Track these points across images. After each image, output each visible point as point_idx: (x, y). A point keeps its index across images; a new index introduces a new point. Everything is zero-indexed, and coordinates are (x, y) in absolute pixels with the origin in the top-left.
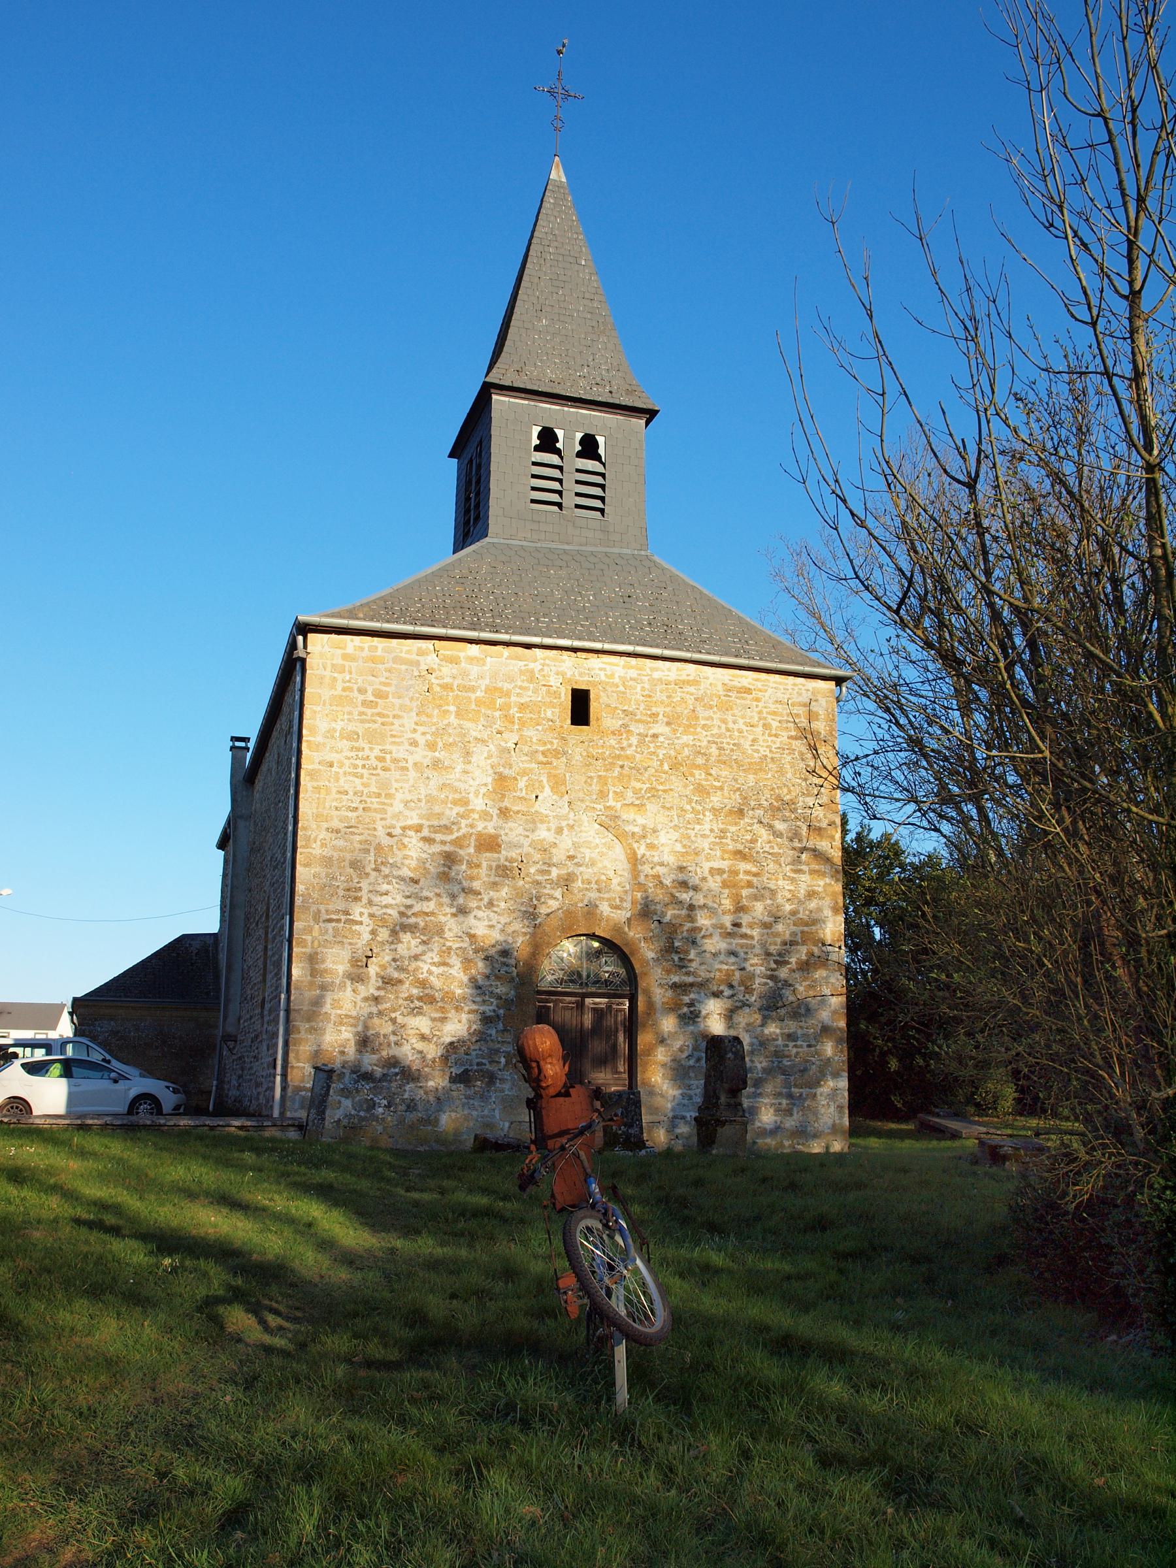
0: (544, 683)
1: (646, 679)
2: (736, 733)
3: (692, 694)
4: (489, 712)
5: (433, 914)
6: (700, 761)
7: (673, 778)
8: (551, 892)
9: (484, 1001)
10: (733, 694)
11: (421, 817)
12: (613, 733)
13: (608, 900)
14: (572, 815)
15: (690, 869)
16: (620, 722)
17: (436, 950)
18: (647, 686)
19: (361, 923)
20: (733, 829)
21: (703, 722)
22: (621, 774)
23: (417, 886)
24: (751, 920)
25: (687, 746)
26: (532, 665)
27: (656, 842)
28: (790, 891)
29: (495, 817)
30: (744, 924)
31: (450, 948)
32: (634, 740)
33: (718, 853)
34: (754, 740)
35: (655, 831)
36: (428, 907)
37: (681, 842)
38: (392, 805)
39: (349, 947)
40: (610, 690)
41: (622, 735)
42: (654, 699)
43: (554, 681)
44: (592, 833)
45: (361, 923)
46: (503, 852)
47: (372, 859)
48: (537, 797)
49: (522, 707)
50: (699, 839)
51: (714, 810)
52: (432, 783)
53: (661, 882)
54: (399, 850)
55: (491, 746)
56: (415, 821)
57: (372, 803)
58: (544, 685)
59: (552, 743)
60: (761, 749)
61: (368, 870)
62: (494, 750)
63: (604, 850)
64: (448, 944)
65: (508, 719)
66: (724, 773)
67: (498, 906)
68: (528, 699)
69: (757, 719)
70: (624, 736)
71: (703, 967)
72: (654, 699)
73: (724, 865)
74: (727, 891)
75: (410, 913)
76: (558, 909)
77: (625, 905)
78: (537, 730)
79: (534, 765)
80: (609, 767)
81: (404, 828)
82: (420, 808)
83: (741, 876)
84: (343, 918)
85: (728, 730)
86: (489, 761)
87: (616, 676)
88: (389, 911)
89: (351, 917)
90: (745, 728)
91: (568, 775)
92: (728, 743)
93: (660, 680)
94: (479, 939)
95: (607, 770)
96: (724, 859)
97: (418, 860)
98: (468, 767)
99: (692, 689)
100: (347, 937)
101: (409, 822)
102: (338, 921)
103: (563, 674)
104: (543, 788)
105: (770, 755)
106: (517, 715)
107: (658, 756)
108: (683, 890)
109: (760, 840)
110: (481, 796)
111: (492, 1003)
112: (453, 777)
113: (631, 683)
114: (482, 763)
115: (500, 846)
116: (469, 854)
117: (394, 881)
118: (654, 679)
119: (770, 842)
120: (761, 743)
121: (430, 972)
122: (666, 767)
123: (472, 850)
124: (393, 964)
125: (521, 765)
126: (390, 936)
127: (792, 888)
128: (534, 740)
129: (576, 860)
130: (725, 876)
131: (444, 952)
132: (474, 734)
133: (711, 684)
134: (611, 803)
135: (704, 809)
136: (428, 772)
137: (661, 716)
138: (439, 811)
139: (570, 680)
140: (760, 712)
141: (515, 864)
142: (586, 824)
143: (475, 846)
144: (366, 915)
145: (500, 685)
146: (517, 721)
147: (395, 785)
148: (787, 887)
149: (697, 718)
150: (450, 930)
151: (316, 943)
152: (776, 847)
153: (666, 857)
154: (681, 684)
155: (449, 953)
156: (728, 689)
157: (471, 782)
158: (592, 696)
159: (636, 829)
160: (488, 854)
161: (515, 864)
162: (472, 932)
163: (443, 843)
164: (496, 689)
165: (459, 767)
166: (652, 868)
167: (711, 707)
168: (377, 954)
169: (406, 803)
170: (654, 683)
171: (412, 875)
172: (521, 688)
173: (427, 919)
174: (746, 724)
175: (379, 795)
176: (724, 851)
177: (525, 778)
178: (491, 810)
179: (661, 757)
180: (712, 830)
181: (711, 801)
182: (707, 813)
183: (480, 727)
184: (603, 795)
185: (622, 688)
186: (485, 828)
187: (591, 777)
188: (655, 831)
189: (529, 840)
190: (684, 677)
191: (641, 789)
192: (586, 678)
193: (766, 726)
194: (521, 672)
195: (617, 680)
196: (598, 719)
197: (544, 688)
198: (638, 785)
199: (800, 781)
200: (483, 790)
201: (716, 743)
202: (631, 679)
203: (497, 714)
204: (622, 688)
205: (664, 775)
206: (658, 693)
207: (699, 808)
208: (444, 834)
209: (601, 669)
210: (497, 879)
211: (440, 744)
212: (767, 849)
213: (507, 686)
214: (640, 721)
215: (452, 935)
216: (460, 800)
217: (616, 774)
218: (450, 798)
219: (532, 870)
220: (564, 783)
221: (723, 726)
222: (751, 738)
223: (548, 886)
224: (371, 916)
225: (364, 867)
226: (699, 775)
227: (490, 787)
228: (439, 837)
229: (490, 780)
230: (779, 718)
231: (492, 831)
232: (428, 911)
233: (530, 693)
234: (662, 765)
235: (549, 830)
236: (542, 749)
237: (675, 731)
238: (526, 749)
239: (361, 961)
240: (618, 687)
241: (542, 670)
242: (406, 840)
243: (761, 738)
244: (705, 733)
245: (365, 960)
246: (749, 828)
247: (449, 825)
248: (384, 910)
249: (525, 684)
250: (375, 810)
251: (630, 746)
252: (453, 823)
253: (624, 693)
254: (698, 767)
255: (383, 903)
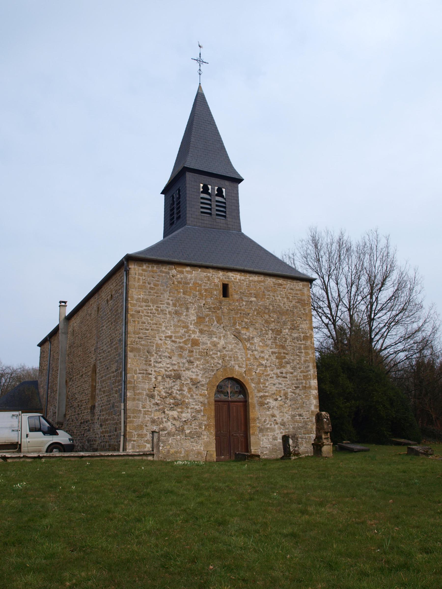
0: (213, 281)
1: (247, 280)
2: (278, 301)
3: (263, 286)
4: (195, 292)
5: (177, 370)
6: (267, 311)
7: (258, 317)
8: (218, 361)
9: (196, 404)
10: (276, 286)
11: (171, 332)
12: (237, 300)
13: (238, 364)
14: (224, 332)
15: (265, 352)
16: (239, 297)
17: (178, 384)
18: (248, 283)
19: (151, 374)
20: (279, 337)
21: (267, 297)
22: (240, 316)
23: (171, 360)
24: (286, 371)
25: (262, 305)
26: (209, 274)
27: (253, 342)
28: (298, 360)
29: (198, 333)
30: (284, 373)
31: (183, 384)
32: (244, 303)
33: (274, 346)
34: (284, 303)
35: (253, 338)
36: (175, 368)
37: (262, 342)
38: (161, 328)
39: (147, 384)
40: (235, 284)
41: (240, 301)
42: (250, 288)
43: (216, 281)
44: (231, 338)
45: (151, 374)
46: (201, 346)
47: (154, 348)
48: (212, 324)
49: (206, 290)
50: (268, 341)
51: (271, 330)
52: (175, 319)
53: (256, 357)
54: (164, 345)
55: (196, 305)
56: (170, 334)
57: (154, 327)
58: (213, 282)
59: (216, 304)
60: (287, 307)
61: (153, 353)
62: (196, 307)
63: (236, 345)
64: (183, 382)
65: (201, 294)
66: (275, 316)
67: (200, 367)
68: (208, 287)
69: (284, 295)
70: (241, 301)
71: (271, 389)
72: (250, 288)
73: (276, 350)
74: (277, 360)
75: (169, 370)
76: (221, 368)
77: (243, 366)
78: (211, 299)
79: (210, 313)
80: (237, 313)
81: (166, 337)
82: (171, 329)
83: (282, 355)
84: (145, 372)
85: (275, 299)
86: (195, 311)
87: (237, 279)
88: (161, 369)
89: (148, 372)
90: (281, 299)
91: (222, 316)
92: (276, 305)
93: (252, 280)
94: (194, 380)
95: (236, 315)
96: (276, 348)
97: (171, 349)
98: (188, 313)
99: (263, 284)
100: (146, 380)
101: (167, 335)
102: (143, 373)
103: (219, 278)
104: (214, 321)
105: (289, 309)
106: (204, 293)
107: (252, 309)
108: (263, 360)
109: (288, 341)
110: (192, 324)
111: (199, 405)
112: (182, 318)
113: (242, 282)
114: (193, 312)
115: (200, 344)
116: (189, 347)
117: (163, 357)
118: (250, 280)
119: (291, 342)
120: (286, 304)
121: (177, 393)
122: (255, 313)
123: (190, 345)
124: (163, 390)
125: (206, 312)
126: (162, 379)
127: (299, 359)
128: (210, 303)
129: (226, 349)
130: (277, 354)
131: (181, 385)
132: (189, 300)
133: (269, 282)
134: (238, 327)
135: (269, 329)
136: (174, 316)
137: (253, 294)
138: (178, 330)
139: (222, 280)
140: (286, 293)
141: (205, 351)
142: (229, 335)
143: (191, 344)
144: (153, 371)
145: (198, 282)
146: (204, 296)
147: (162, 320)
148: (298, 359)
149: (265, 295)
150: (183, 376)
151: (136, 382)
152: (293, 343)
153: (257, 347)
154: (260, 282)
155: (183, 386)
156: (275, 284)
157: (189, 319)
158: (230, 286)
159: (246, 337)
160: (196, 347)
161: (205, 351)
162: (191, 377)
163: (180, 343)
164: (197, 283)
165: (184, 314)
166: (252, 352)
167: (269, 291)
168: (158, 386)
169: (166, 327)
170: (250, 282)
171: (169, 355)
172: (205, 283)
173: (175, 372)
174: (281, 297)
175: (156, 324)
176: (276, 345)
177: (208, 318)
178: (196, 330)
179: (253, 309)
180: (272, 337)
181: (271, 326)
182: (270, 331)
183: (191, 298)
184: (235, 324)
185: (239, 284)
186: (194, 337)
187: (230, 317)
188: (253, 338)
189: (210, 341)
190: (260, 279)
191: (247, 322)
192: (227, 280)
193: (288, 298)
194: (205, 277)
195: (238, 280)
196: (232, 295)
197: (213, 283)
198: (246, 320)
199: (300, 319)
200: (193, 322)
201: (272, 304)
202: (243, 280)
203: (197, 293)
204: (239, 284)
205: (255, 317)
206: (252, 286)
207: (267, 329)
208: (180, 339)
209: (232, 276)
210: (199, 356)
211: (178, 305)
212: (290, 344)
213: (200, 282)
214: (246, 296)
215: (184, 378)
216: (185, 326)
217: (239, 316)
218: (182, 325)
219: (211, 353)
220: (221, 319)
221: (274, 298)
222: (283, 302)
223: (217, 359)
224: (155, 371)
225: (152, 352)
226: (267, 316)
227: (196, 321)
228: (178, 340)
229: (195, 318)
230: (292, 295)
231: (197, 338)
232: (175, 369)
233: (208, 285)
234: (254, 312)
235: (216, 337)
236: (213, 306)
237: (258, 300)
238: (208, 307)
239: (152, 389)
240: (238, 283)
241: (212, 276)
242: (167, 342)
243: (286, 302)
244: (268, 301)
245: (153, 388)
246: (284, 336)
247: (181, 335)
248: (160, 369)
249: (207, 282)
250: (156, 330)
251: (243, 305)
252: (183, 335)
253: (240, 285)
254: (266, 314)
255: (159, 366)
